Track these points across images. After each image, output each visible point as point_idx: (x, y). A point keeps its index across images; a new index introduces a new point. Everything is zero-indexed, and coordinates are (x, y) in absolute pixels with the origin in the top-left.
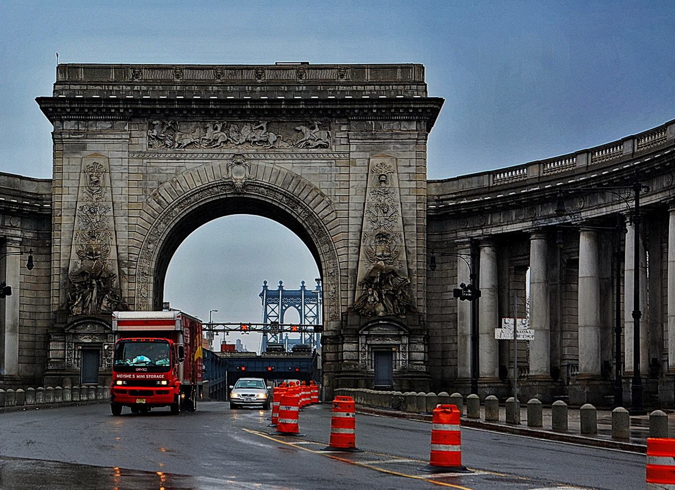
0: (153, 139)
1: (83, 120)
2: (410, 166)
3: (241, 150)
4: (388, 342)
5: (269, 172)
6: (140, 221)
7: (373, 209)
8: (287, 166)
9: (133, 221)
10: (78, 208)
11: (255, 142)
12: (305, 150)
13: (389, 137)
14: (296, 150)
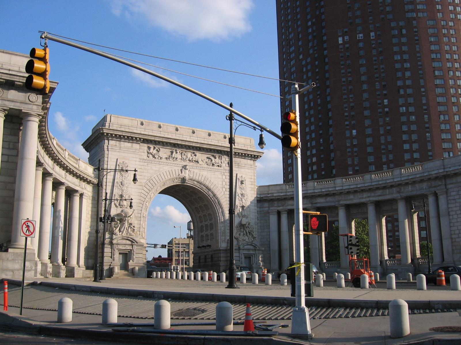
0: (149, 154)
1: (118, 141)
2: (251, 179)
3: (187, 163)
4: (251, 253)
5: (198, 175)
6: (143, 191)
7: (240, 195)
8: (205, 173)
9: (140, 191)
10: (115, 182)
11: (192, 161)
12: (212, 167)
13: (244, 165)
14: (208, 167)
